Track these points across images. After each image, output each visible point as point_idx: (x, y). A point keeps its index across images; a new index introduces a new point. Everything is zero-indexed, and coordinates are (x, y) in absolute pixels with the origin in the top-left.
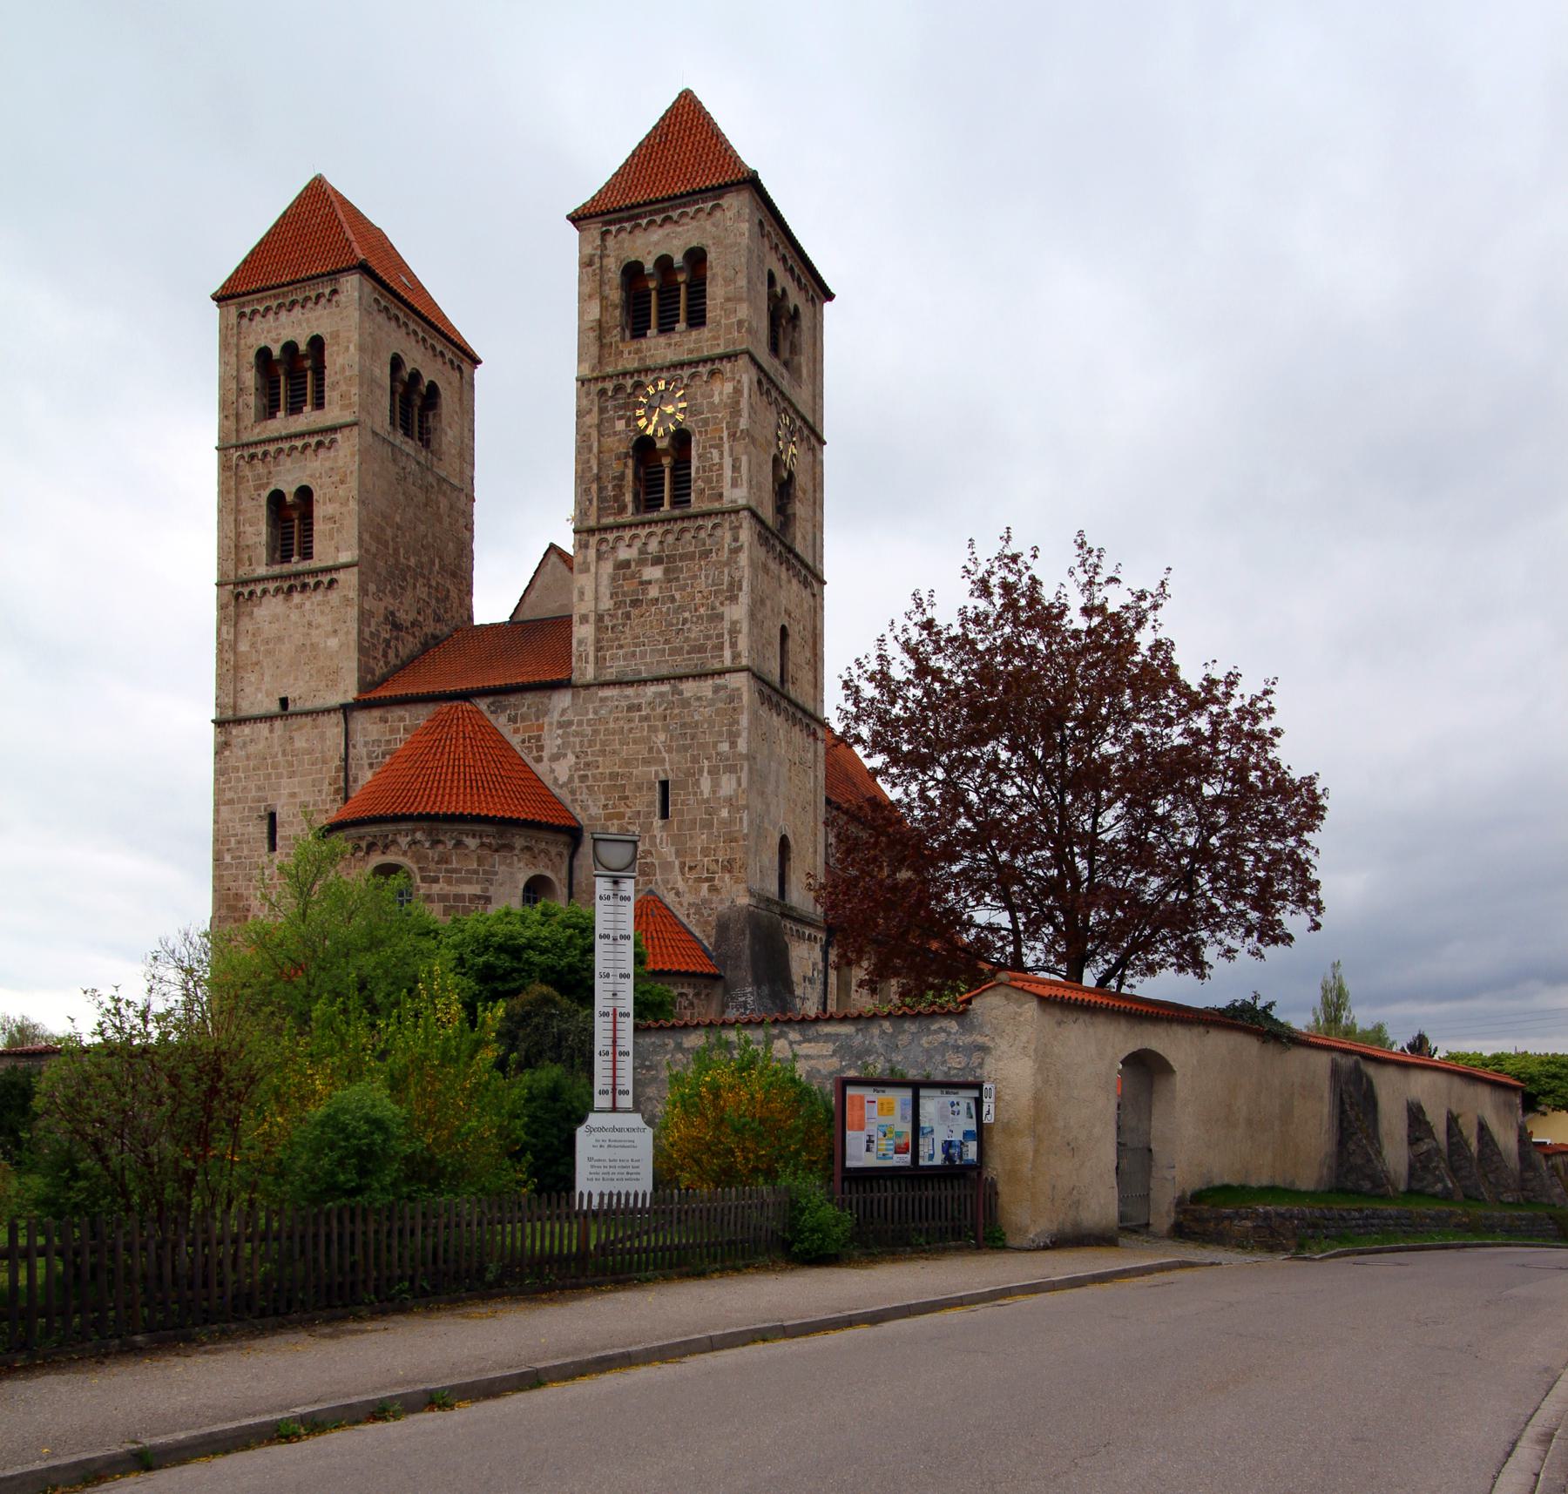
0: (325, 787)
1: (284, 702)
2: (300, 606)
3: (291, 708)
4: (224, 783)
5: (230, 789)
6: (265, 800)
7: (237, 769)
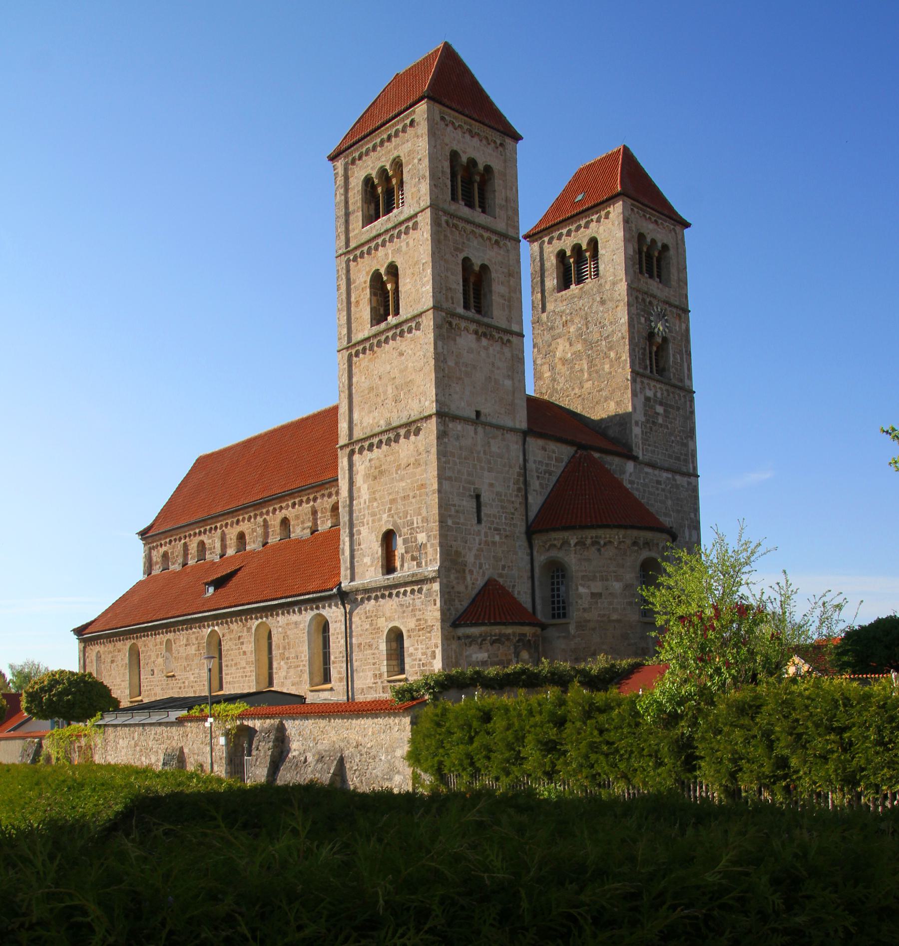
0: (511, 484)
1: (478, 413)
2: (486, 349)
3: (483, 418)
4: (445, 462)
5: (449, 468)
6: (474, 484)
7: (453, 454)
